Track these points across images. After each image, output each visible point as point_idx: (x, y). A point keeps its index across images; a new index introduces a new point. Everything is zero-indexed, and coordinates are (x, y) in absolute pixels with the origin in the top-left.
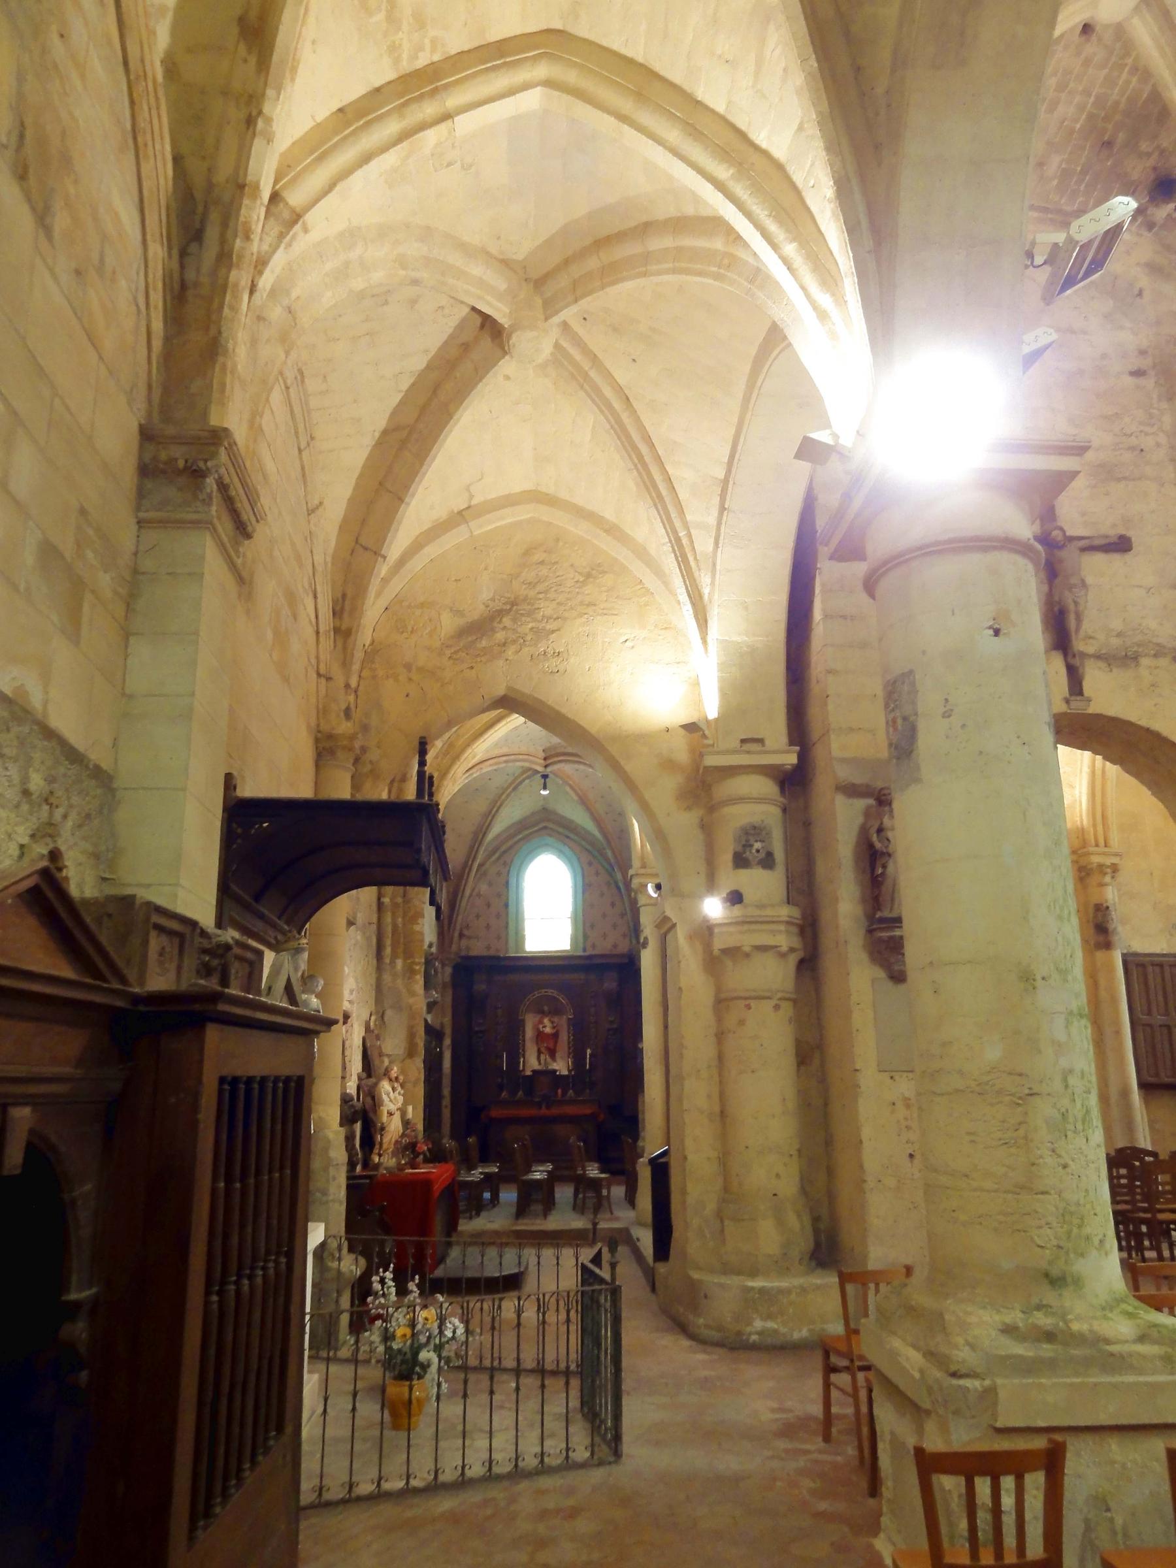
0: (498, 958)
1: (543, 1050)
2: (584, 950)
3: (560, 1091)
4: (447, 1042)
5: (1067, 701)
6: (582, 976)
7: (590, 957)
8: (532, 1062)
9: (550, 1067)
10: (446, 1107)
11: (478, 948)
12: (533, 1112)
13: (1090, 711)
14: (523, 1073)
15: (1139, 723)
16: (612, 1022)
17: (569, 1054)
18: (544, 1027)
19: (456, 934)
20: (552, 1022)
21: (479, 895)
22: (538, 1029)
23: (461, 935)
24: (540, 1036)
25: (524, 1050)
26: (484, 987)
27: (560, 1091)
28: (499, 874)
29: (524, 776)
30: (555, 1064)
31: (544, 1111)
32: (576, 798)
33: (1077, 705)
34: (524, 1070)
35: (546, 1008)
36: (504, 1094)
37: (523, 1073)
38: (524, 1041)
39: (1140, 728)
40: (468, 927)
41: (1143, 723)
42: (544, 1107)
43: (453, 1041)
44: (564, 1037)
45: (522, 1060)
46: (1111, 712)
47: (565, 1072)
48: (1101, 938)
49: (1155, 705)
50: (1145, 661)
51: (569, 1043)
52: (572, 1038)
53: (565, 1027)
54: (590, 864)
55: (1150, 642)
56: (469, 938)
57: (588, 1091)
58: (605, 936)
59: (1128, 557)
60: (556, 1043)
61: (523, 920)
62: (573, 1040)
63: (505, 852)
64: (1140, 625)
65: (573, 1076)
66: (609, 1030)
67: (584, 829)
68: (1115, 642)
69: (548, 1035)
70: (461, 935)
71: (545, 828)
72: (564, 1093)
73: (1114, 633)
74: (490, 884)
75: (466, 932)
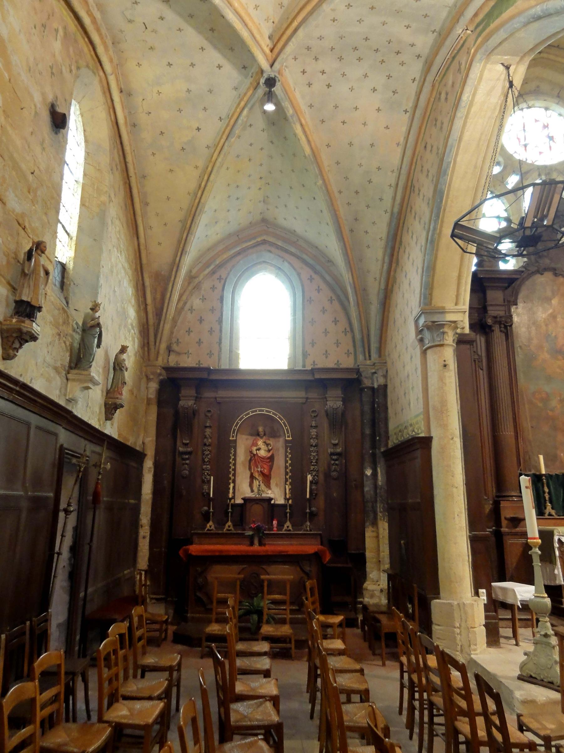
0: (208, 370)
1: (256, 475)
2: (304, 366)
3: (275, 522)
4: (149, 464)
6: (302, 394)
7: (312, 371)
8: (231, 438)
9: (264, 495)
10: (144, 537)
11: (188, 362)
12: (242, 548)
14: (232, 501)
16: (335, 445)
17: (286, 480)
18: (259, 449)
19: (163, 346)
20: (267, 445)
21: (191, 310)
22: (251, 452)
23: (169, 350)
24: (253, 459)
25: (234, 475)
26: (191, 403)
27: (275, 522)
28: (213, 288)
29: (242, 104)
30: (270, 492)
31: (256, 547)
32: (308, 151)
34: (234, 497)
35: (261, 429)
36: (211, 525)
37: (232, 501)
38: (235, 465)
40: (178, 342)
42: (256, 541)
43: (157, 465)
44: (280, 462)
45: (231, 486)
47: (281, 501)
51: (286, 467)
52: (290, 462)
53: (282, 452)
54: (311, 279)
56: (178, 354)
57: (308, 523)
58: (326, 354)
60: (271, 468)
61: (238, 339)
62: (290, 465)
63: (220, 266)
65: (290, 505)
66: (332, 454)
67: (306, 241)
69: (263, 458)
70: (169, 350)
71: (264, 242)
72: (281, 525)
74: (204, 299)
75: (175, 347)
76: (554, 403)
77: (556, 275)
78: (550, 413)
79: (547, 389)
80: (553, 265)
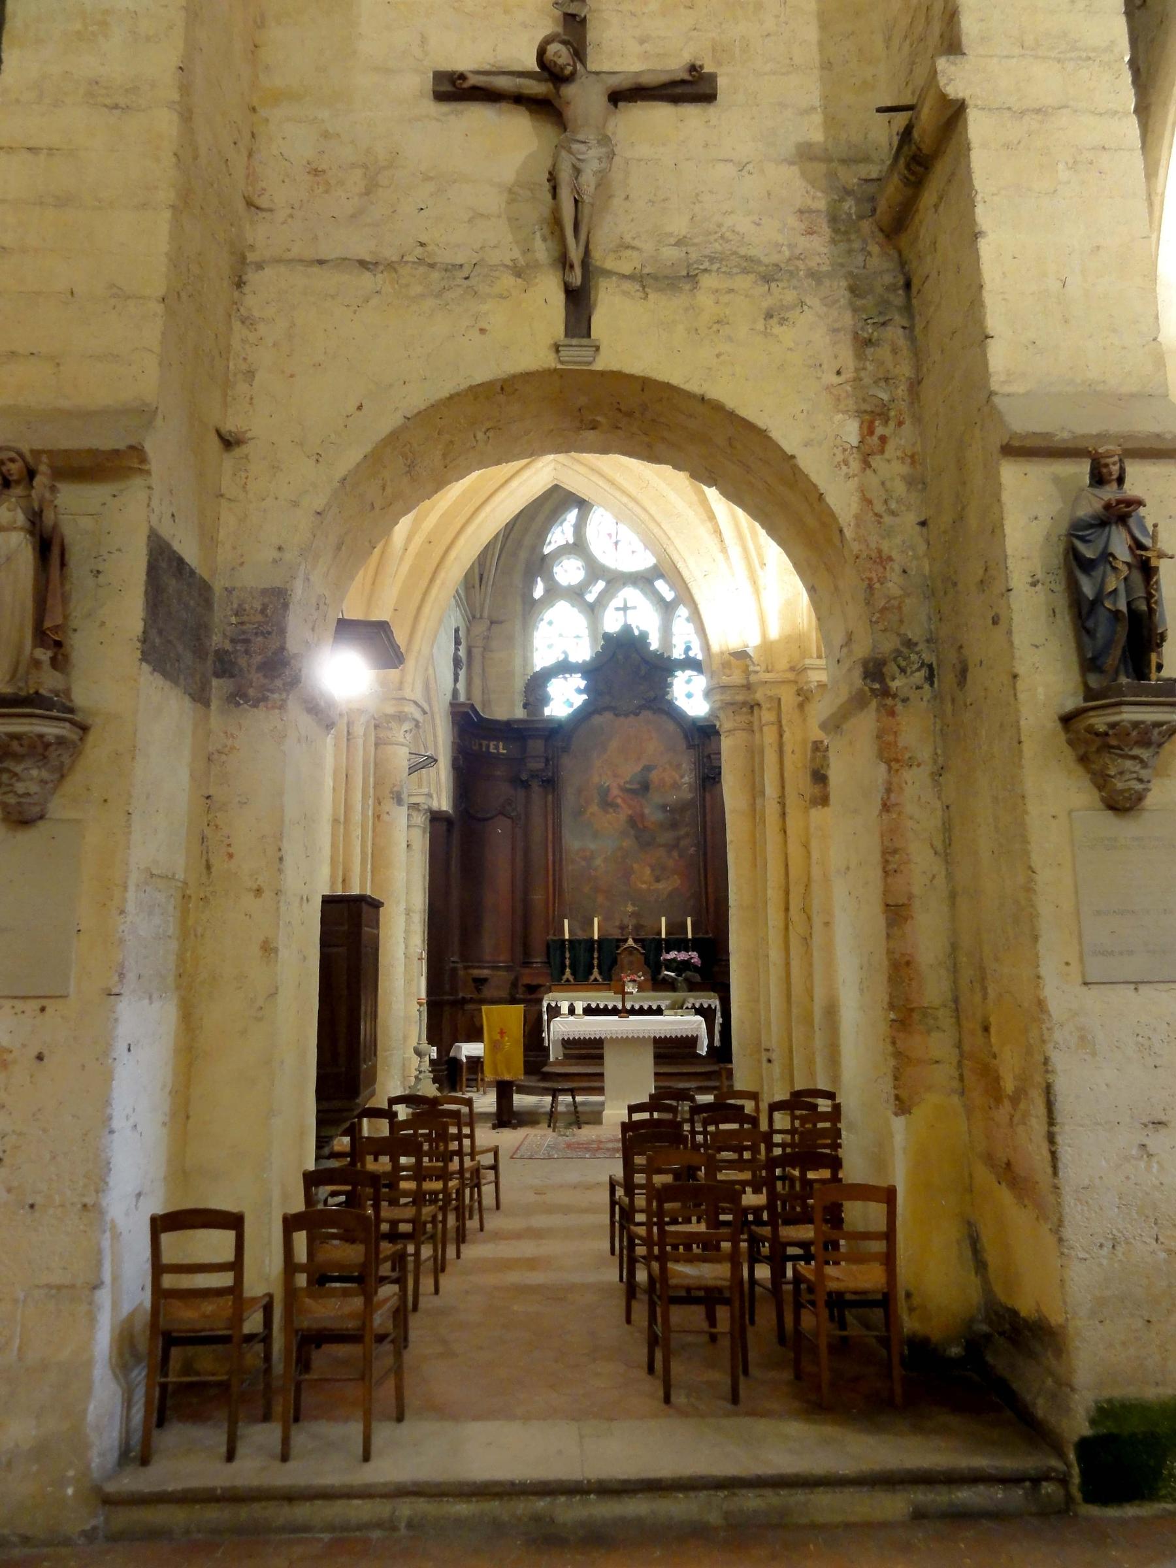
5: (557, 348)
13: (600, 365)
15: (687, 387)
33: (575, 355)
39: (689, 395)
41: (693, 387)
46: (636, 366)
48: (817, 790)
49: (718, 356)
50: (707, 281)
55: (735, 253)
59: (711, 111)
64: (720, 226)
68: (670, 254)
73: (673, 241)
76: (598, 862)
77: (616, 715)
78: (593, 873)
79: (592, 846)
80: (613, 704)
